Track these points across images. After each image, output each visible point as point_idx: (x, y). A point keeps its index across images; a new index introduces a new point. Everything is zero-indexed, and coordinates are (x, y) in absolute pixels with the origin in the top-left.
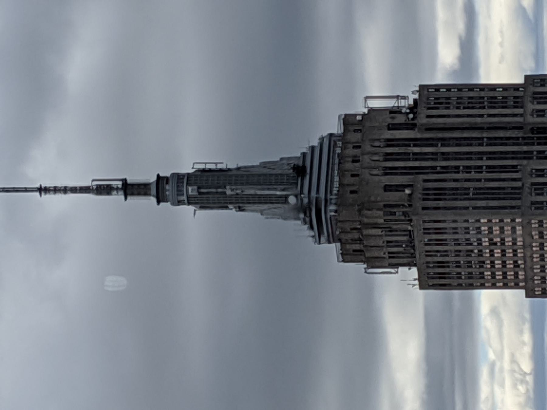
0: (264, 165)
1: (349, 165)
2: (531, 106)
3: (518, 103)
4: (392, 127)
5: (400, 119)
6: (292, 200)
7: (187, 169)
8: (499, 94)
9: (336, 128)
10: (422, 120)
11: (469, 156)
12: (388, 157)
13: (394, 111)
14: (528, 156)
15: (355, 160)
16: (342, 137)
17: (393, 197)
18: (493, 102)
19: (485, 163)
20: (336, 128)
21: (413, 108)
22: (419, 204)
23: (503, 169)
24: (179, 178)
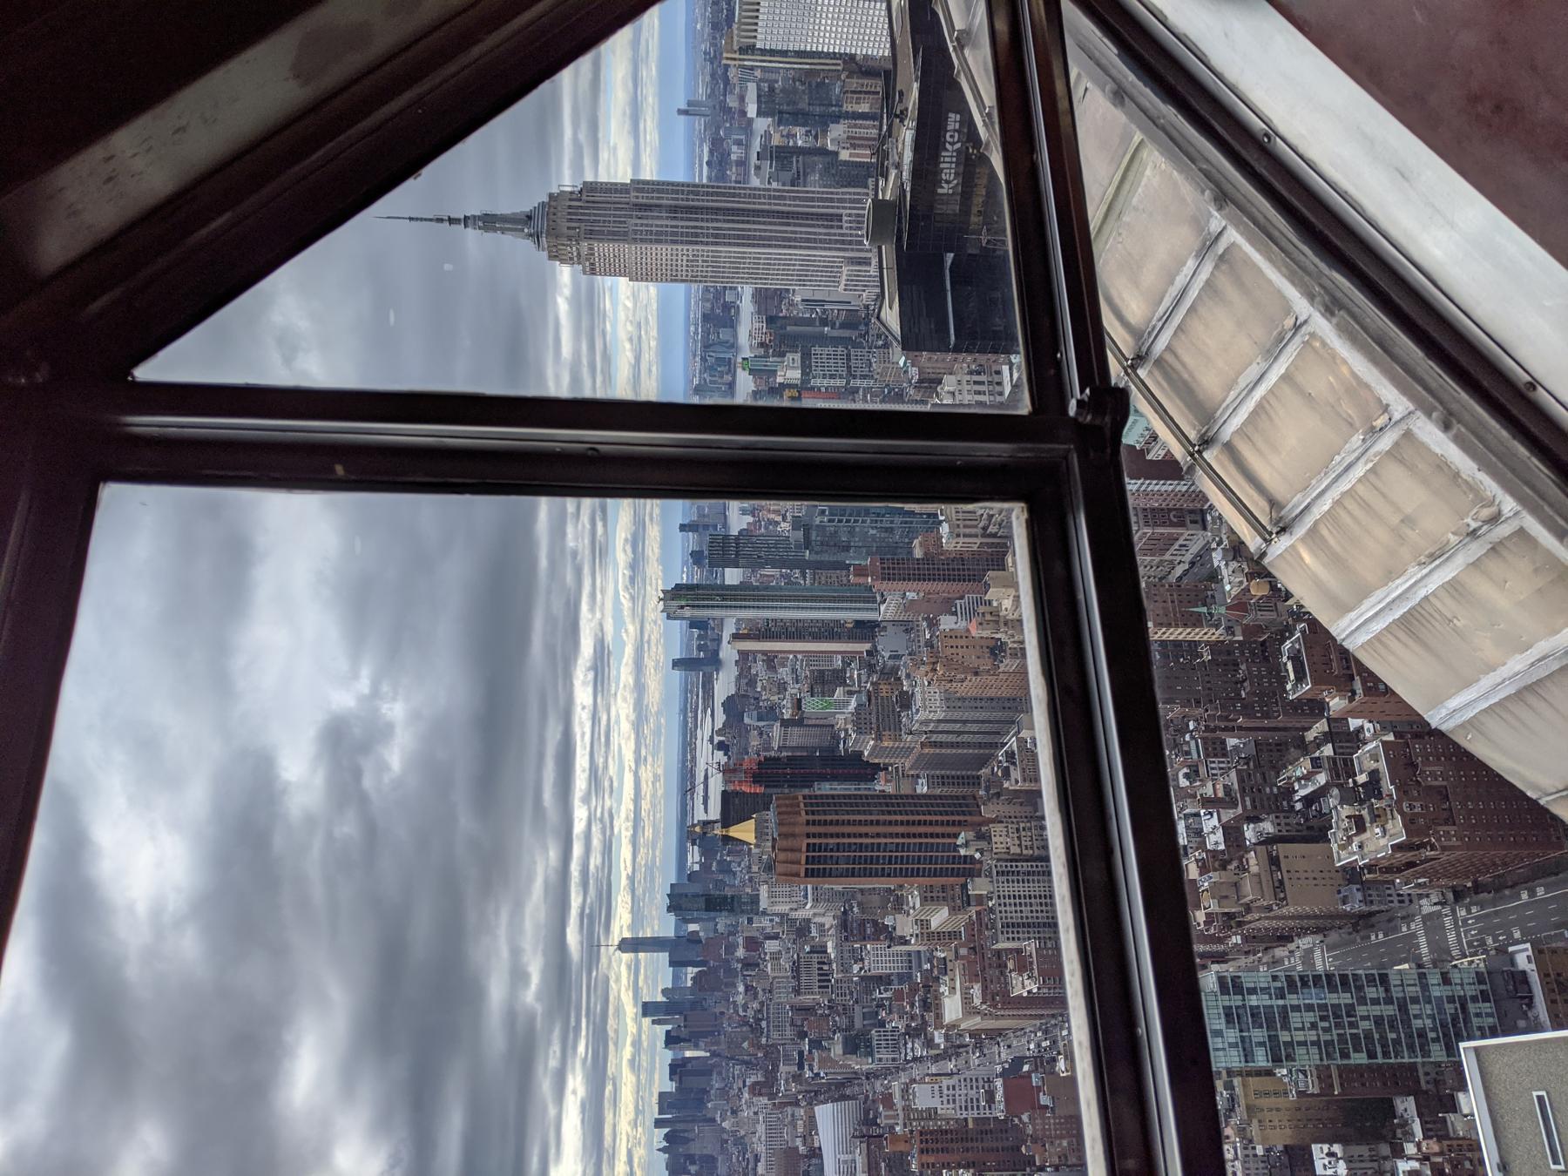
0: (513, 214)
1: (551, 217)
2: (633, 194)
3: (627, 192)
4: (570, 200)
5: (574, 196)
6: (526, 230)
7: (478, 213)
8: (619, 187)
9: (546, 199)
10: (584, 198)
11: (605, 215)
12: (569, 214)
13: (572, 193)
14: (631, 217)
15: (554, 214)
16: (549, 203)
17: (572, 232)
18: (616, 191)
19: (612, 219)
20: (546, 199)
21: (580, 192)
22: (583, 236)
23: (620, 222)
24: (474, 217)
